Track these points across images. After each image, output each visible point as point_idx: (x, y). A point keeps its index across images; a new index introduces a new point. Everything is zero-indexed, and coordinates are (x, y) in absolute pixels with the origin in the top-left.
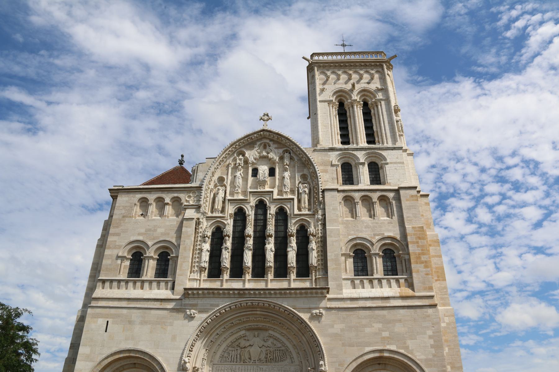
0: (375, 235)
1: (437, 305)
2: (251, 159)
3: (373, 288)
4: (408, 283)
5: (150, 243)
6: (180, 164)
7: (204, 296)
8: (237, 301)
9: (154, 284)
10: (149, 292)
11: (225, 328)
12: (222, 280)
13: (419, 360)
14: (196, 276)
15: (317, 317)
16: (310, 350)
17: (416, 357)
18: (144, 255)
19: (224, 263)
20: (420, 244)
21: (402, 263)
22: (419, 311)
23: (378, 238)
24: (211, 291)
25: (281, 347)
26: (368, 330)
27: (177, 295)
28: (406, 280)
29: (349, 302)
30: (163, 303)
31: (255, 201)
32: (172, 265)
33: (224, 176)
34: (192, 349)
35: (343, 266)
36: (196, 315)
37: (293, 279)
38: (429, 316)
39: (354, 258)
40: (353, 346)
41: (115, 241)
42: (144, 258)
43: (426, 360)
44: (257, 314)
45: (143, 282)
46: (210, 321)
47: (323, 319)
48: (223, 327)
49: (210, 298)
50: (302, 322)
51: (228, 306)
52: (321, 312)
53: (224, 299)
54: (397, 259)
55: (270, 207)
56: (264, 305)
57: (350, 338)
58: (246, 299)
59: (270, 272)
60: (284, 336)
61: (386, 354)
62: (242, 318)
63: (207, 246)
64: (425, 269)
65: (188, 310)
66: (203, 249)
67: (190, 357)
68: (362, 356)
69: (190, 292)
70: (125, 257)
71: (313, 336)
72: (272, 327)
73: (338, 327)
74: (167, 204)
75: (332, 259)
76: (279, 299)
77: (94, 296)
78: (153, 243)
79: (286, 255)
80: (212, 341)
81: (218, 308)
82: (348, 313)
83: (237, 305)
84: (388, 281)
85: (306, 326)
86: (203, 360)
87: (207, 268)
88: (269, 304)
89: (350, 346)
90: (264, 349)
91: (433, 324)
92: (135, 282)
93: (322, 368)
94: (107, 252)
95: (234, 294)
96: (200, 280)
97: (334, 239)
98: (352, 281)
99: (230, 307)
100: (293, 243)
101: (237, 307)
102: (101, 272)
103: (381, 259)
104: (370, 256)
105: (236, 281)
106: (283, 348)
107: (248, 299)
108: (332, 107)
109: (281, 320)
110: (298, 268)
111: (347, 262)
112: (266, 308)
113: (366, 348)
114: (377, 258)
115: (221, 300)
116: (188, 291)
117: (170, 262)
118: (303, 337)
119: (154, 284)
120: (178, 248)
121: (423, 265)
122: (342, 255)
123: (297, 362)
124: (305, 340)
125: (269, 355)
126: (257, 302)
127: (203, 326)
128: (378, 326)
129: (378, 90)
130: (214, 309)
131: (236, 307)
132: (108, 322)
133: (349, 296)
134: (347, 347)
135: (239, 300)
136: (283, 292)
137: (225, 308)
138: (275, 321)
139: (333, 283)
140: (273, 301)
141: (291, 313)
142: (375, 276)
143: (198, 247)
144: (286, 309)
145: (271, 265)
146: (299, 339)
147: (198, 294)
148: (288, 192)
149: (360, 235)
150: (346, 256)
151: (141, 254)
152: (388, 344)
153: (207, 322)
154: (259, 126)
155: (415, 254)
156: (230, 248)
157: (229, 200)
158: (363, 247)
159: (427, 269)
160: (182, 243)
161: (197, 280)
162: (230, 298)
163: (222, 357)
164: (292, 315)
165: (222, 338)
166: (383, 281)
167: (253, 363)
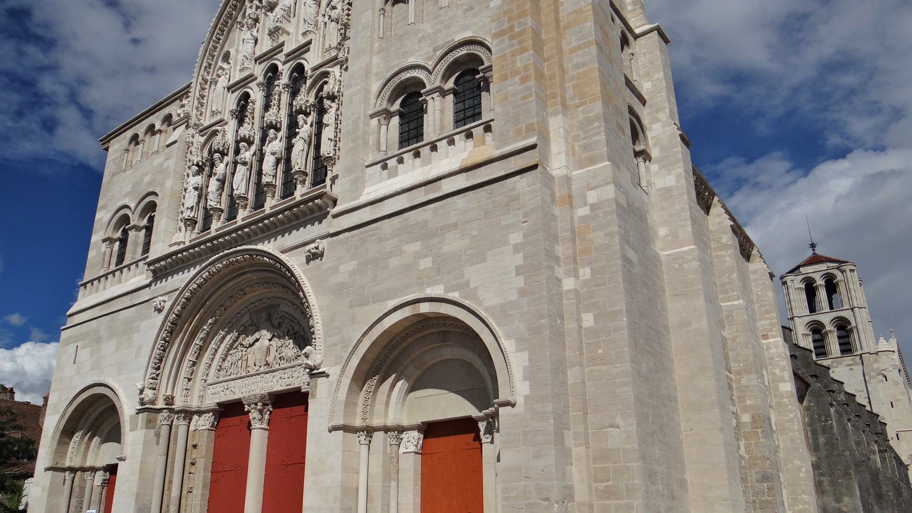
0: (435, 50)
5: (132, 206)
20: (517, 30)
23: (439, 53)
26: (394, 262)
33: (230, 50)
35: (372, 139)
38: (516, 198)
40: (367, 304)
43: (503, 311)
55: (282, 73)
61: (424, 308)
64: (521, 87)
74: (160, 131)
75: (348, 131)
91: (526, 215)
99: (201, 276)
103: (450, 98)
111: (384, 128)
121: (517, 78)
122: (372, 116)
128: (414, 247)
148: (307, 31)
149: (412, 61)
153: (174, 313)
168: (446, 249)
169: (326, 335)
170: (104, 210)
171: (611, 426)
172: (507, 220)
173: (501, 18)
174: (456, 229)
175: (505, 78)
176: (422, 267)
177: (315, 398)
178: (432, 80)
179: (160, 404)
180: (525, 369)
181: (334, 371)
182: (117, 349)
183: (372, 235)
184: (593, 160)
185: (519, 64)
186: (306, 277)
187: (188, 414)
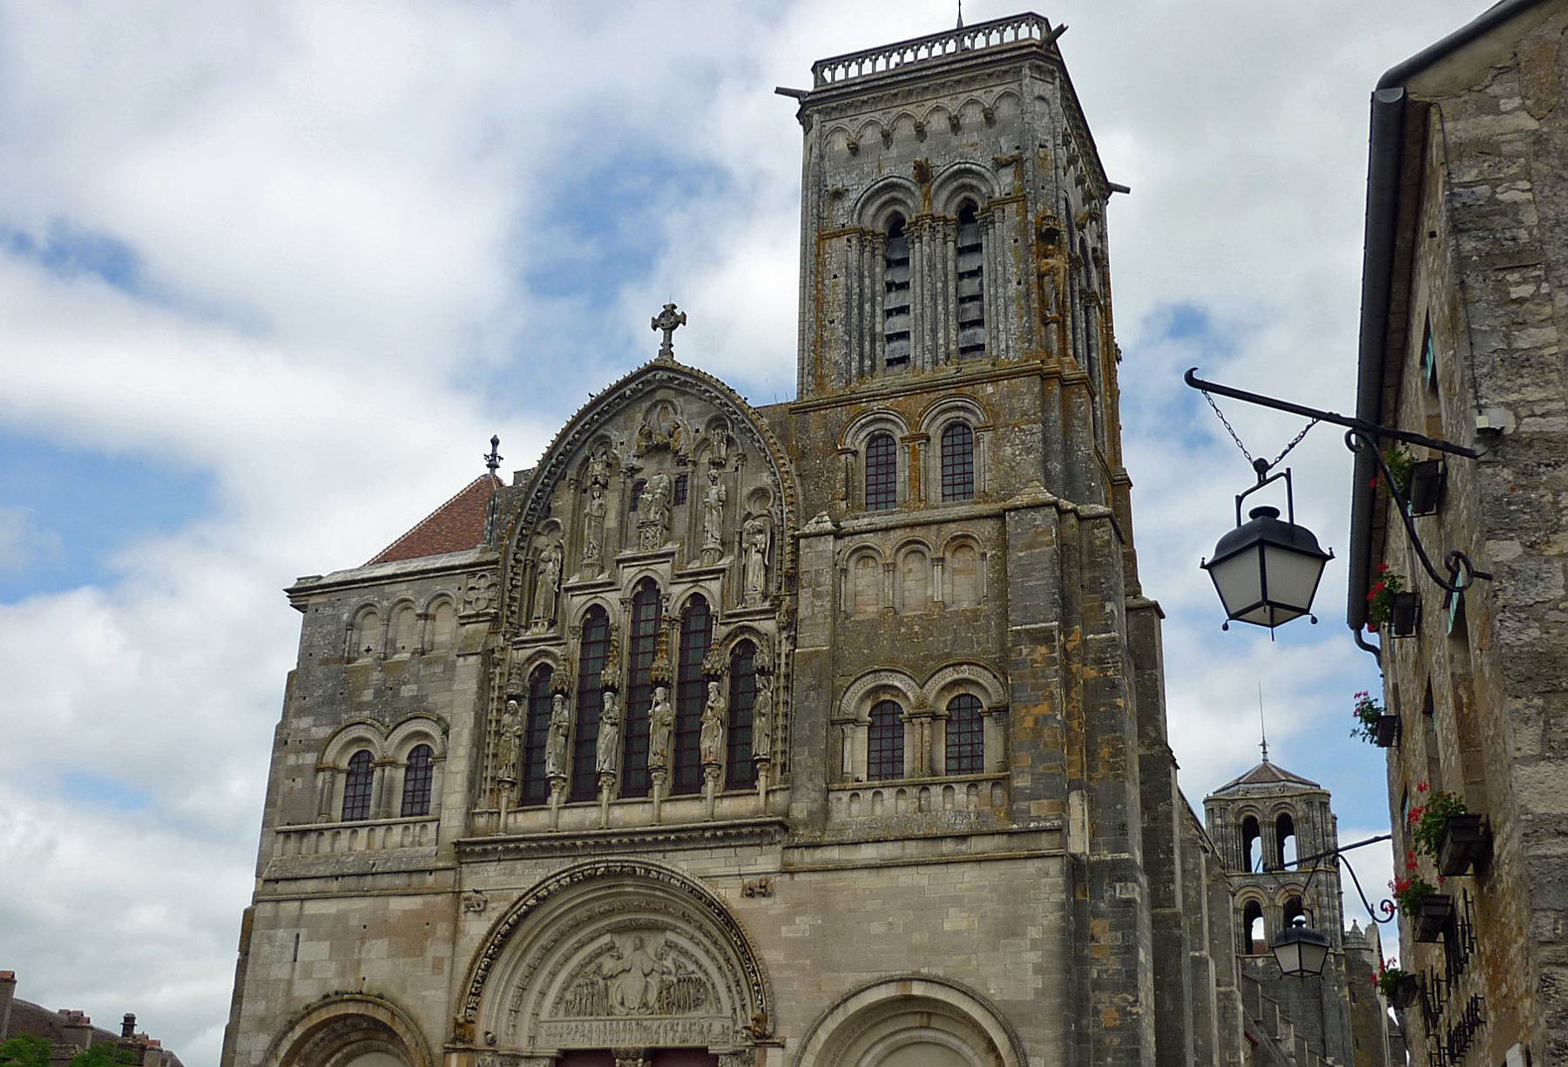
2: (627, 458)
6: (488, 466)
25: (693, 972)
31: (632, 585)
39: (871, 727)
60: (698, 944)
61: (918, 990)
67: (473, 1008)
87: (519, 782)
88: (645, 869)
90: (654, 981)
100: (718, 699)
106: (700, 975)
108: (863, 247)
112: (641, 876)
123: (728, 1011)
125: (664, 993)
127: (499, 933)
129: (1000, 164)
132: (298, 936)
153: (507, 922)
154: (649, 346)
157: (567, 590)
163: (560, 999)
165: (557, 956)
167: (628, 1014)
168: (947, 926)
181: (793, 1044)
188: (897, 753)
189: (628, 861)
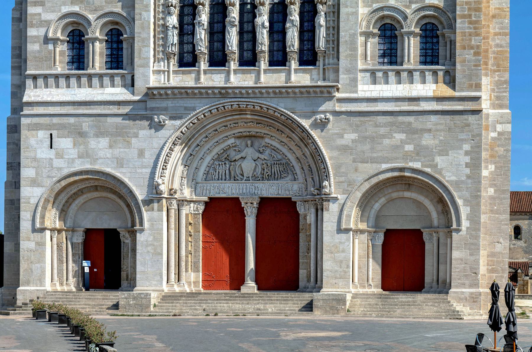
1: (482, 111)
3: (400, 84)
4: (450, 75)
7: (174, 96)
8: (219, 102)
9: (106, 80)
10: (100, 91)
11: (207, 137)
12: (199, 72)
13: (447, 181)
14: (162, 66)
15: (322, 125)
16: (314, 166)
17: (445, 179)
18: (86, 37)
19: (199, 46)
20: (473, 19)
21: (446, 47)
22: (457, 117)
23: (414, 6)
24: (183, 91)
26: (386, 142)
27: (138, 95)
28: (447, 72)
29: (365, 104)
30: (121, 107)
32: (127, 48)
34: (166, 167)
35: (360, 50)
36: (167, 122)
37: (294, 69)
38: (468, 125)
40: (367, 162)
41: (40, 14)
42: (87, 41)
43: (457, 184)
44: (247, 119)
45: (90, 77)
46: (185, 131)
47: (330, 126)
48: (204, 135)
49: (183, 99)
50: (303, 131)
51: (208, 110)
52: (327, 117)
53: (202, 99)
54: (440, 38)
56: (254, 108)
57: (364, 152)
58: (231, 100)
59: (263, 59)
61: (407, 174)
62: (228, 123)
63: (173, 20)
64: (474, 58)
65: (156, 117)
66: (168, 26)
68: (377, 175)
69: (155, 92)
70: (58, 39)
71: (317, 148)
72: (269, 135)
73: (350, 137)
75: (346, 41)
76: (273, 99)
77: (25, 99)
78: (95, 16)
79: (284, 33)
80: (191, 155)
81: (194, 113)
82: (362, 119)
83: (219, 108)
84: (422, 72)
85: (308, 136)
86: (182, 180)
88: (260, 107)
89: (363, 162)
91: (473, 136)
92: (79, 77)
93: (326, 190)
94: (31, 32)
95: (214, 93)
96: (168, 72)
97: (350, 10)
98: (373, 73)
101: (220, 110)
102: (28, 62)
104: (402, 36)
105: (217, 72)
107: (233, 100)
109: (279, 126)
110: (301, 51)
111: (369, 44)
112: (257, 111)
113: (383, 164)
114: (412, 39)
115: (198, 101)
116: (153, 91)
117: (125, 45)
118: (306, 149)
119: (106, 80)
120: (132, 23)
121: (472, 51)
124: (309, 153)
126: (245, 103)
130: (190, 114)
131: (218, 111)
132: (51, 135)
133: (368, 95)
134: (360, 164)
135: (222, 102)
136: (277, 91)
137: (203, 112)
138: (271, 127)
139: (345, 76)
140: (265, 103)
141: (289, 118)
142: (405, 66)
143: (161, 22)
144: (283, 114)
145: (263, 49)
146: (302, 151)
147: (167, 94)
150: (367, 35)
151: (81, 34)
152: (411, 161)
153: (181, 132)
155: (464, 34)
156: (206, 24)
158: (394, 20)
159: (477, 58)
160: (137, 17)
161: (164, 72)
162: (210, 99)
164: (291, 122)
166: (414, 73)
168: (424, 143)
169: (335, 175)
170: (41, 7)
171: (498, 242)
172: (462, 136)
173: (463, 5)
174: (431, 133)
175: (464, 48)
176: (406, 149)
177: (328, 211)
178: (408, 24)
179: (165, 196)
180: (467, 214)
182: (111, 147)
183: (370, 121)
184: (501, 107)
185: (473, 43)
186: (317, 135)
187: (181, 202)
188: (393, 51)
189: (250, 102)
